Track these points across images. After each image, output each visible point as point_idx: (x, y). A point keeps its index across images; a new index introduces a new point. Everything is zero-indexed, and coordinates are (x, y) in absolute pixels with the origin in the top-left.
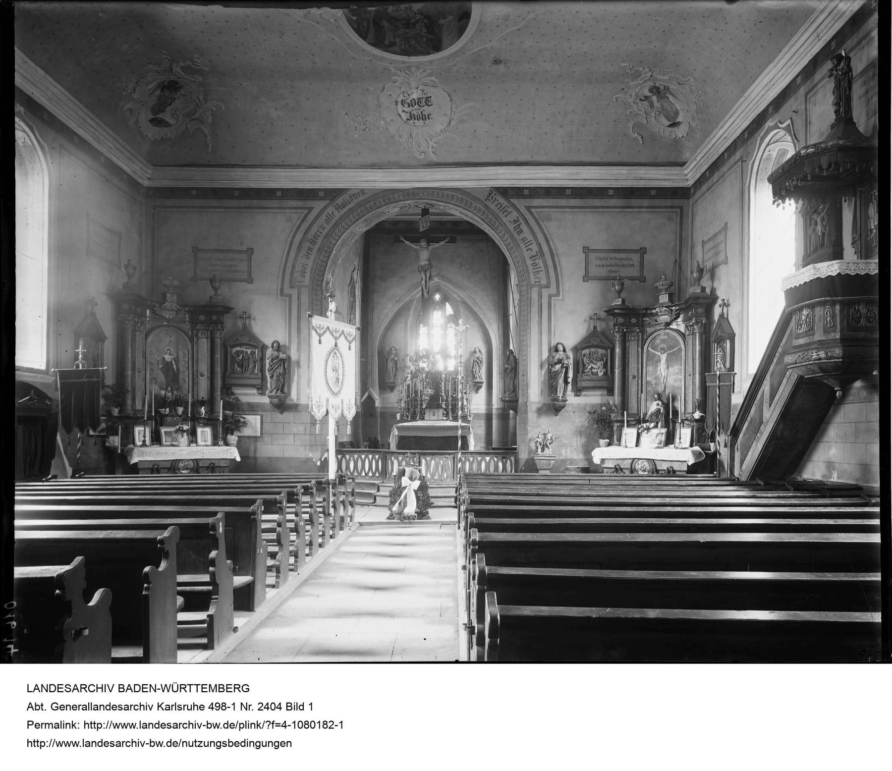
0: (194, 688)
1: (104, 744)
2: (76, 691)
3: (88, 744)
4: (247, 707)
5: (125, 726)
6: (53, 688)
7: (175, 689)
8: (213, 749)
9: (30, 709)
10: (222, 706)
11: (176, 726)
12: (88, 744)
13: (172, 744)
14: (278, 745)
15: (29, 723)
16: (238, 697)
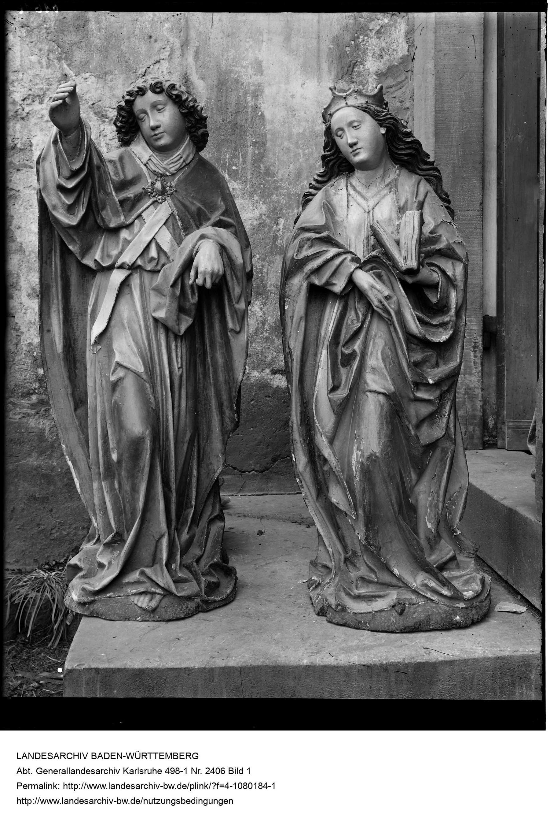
0: (153, 756)
1: (80, 801)
2: (56, 758)
3: (67, 802)
4: (196, 771)
5: (96, 787)
6: (38, 756)
7: (138, 757)
8: (169, 805)
9: (19, 773)
10: (176, 771)
11: (139, 787)
12: (67, 802)
13: (136, 801)
14: (222, 802)
15: (19, 785)
16: (189, 763)
